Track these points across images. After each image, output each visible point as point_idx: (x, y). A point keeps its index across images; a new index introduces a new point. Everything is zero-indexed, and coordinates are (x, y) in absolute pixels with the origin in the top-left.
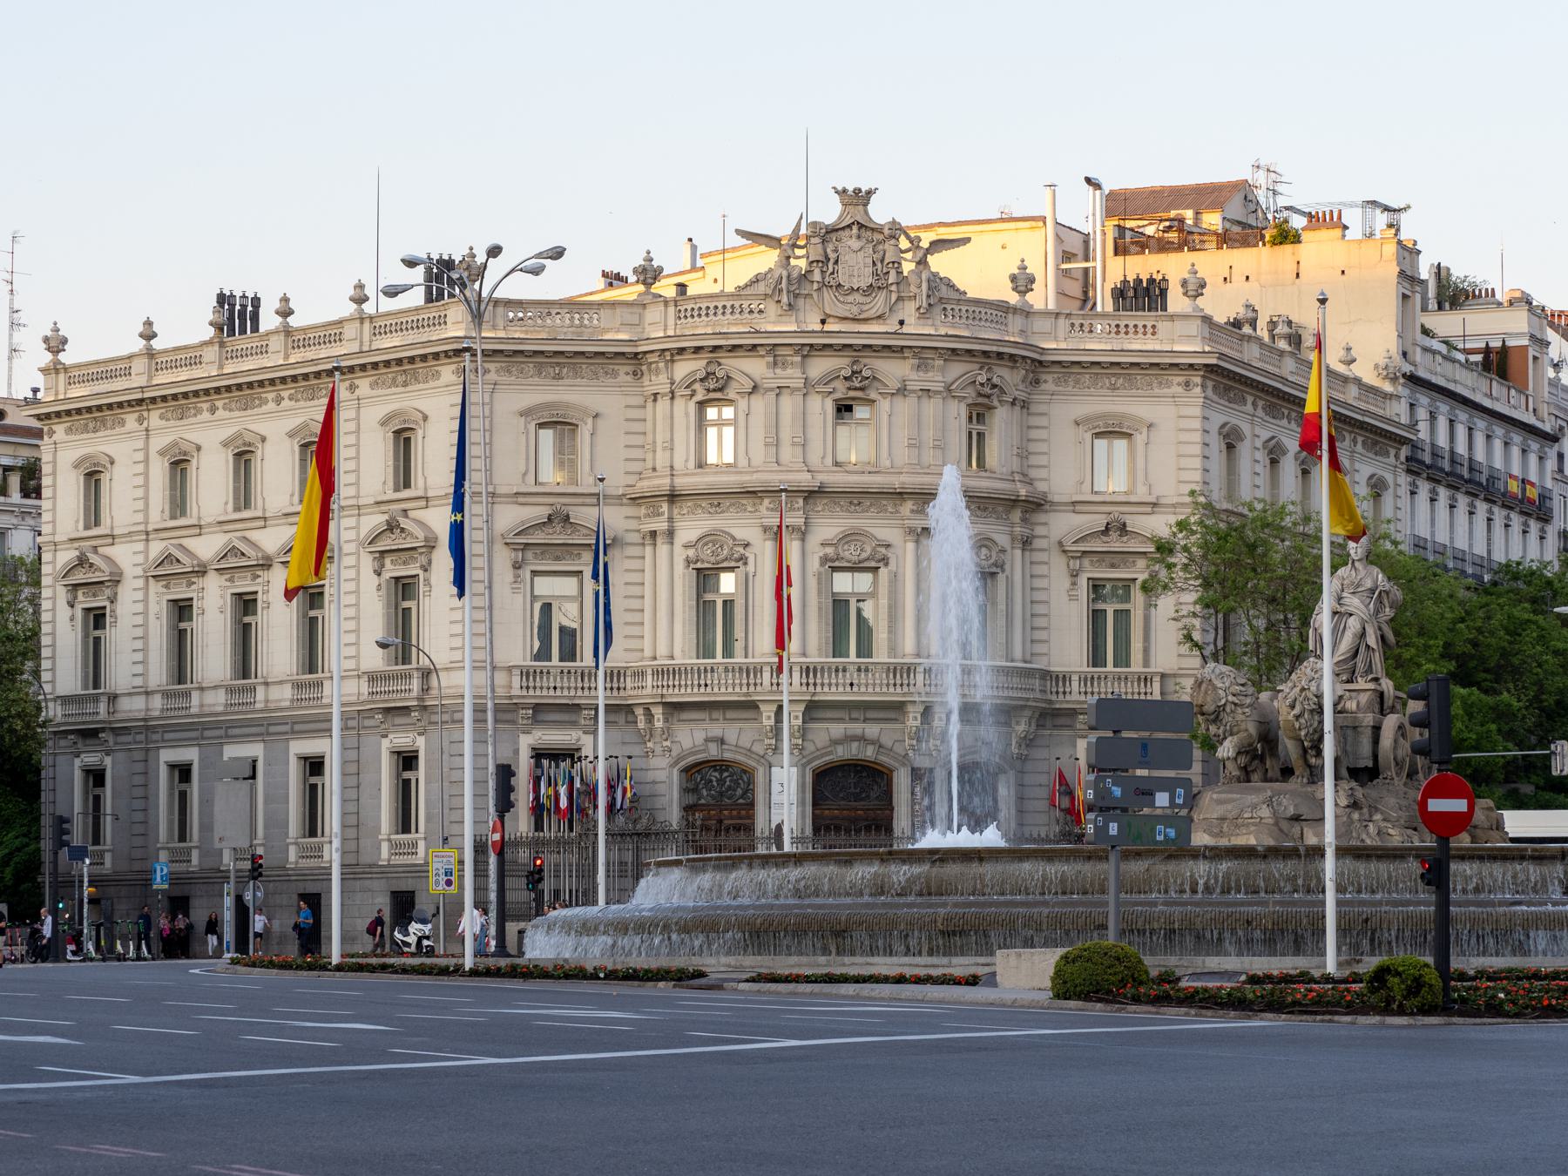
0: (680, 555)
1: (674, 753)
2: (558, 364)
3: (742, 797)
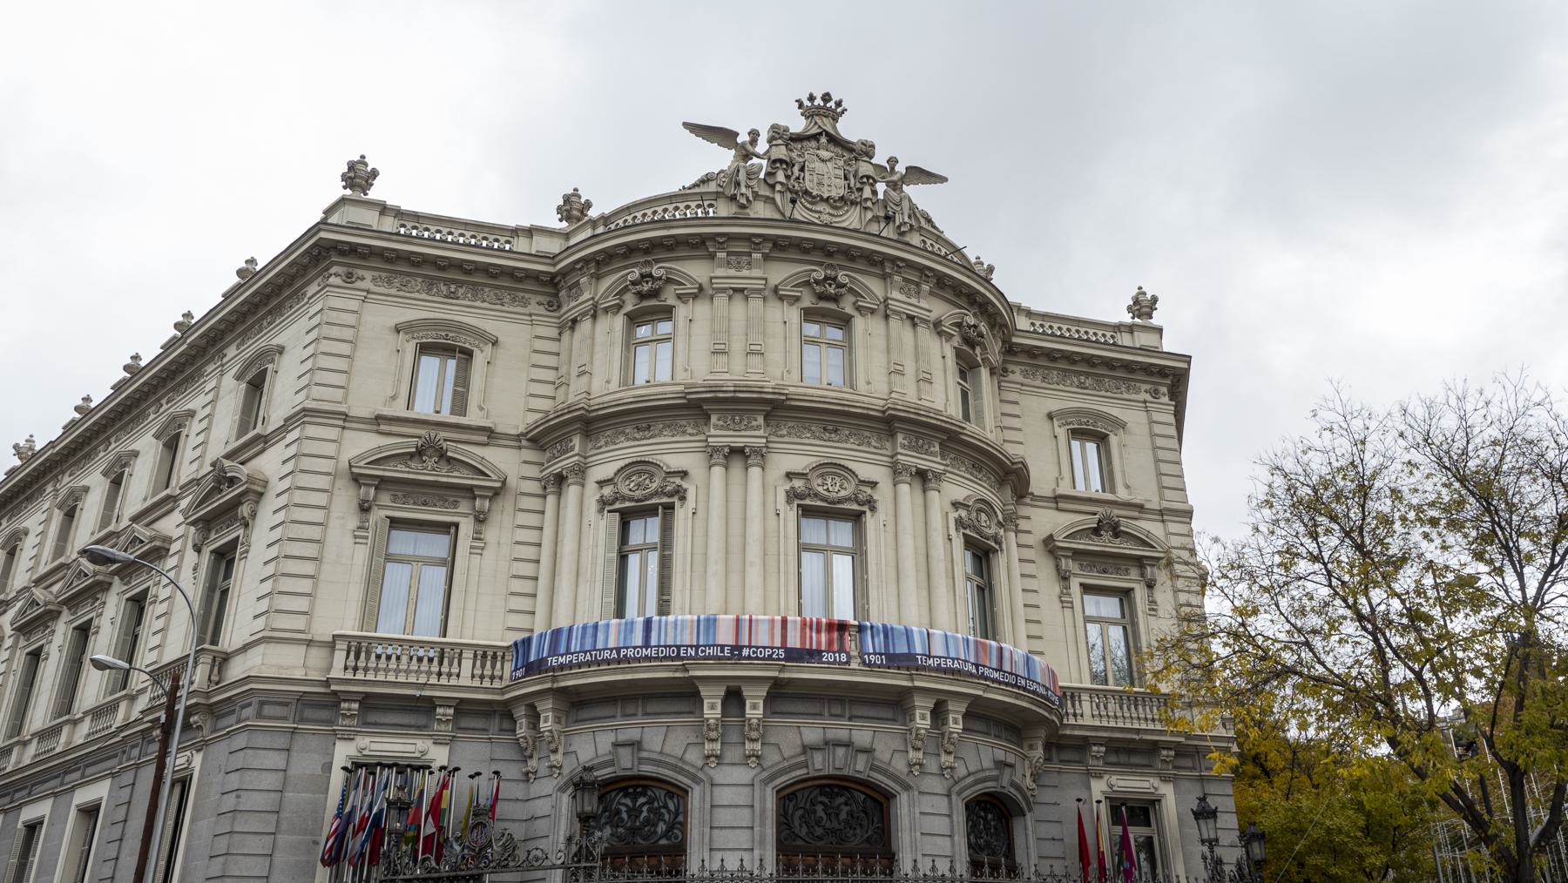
0: (592, 494)
1: (566, 771)
2: (453, 281)
3: (665, 835)
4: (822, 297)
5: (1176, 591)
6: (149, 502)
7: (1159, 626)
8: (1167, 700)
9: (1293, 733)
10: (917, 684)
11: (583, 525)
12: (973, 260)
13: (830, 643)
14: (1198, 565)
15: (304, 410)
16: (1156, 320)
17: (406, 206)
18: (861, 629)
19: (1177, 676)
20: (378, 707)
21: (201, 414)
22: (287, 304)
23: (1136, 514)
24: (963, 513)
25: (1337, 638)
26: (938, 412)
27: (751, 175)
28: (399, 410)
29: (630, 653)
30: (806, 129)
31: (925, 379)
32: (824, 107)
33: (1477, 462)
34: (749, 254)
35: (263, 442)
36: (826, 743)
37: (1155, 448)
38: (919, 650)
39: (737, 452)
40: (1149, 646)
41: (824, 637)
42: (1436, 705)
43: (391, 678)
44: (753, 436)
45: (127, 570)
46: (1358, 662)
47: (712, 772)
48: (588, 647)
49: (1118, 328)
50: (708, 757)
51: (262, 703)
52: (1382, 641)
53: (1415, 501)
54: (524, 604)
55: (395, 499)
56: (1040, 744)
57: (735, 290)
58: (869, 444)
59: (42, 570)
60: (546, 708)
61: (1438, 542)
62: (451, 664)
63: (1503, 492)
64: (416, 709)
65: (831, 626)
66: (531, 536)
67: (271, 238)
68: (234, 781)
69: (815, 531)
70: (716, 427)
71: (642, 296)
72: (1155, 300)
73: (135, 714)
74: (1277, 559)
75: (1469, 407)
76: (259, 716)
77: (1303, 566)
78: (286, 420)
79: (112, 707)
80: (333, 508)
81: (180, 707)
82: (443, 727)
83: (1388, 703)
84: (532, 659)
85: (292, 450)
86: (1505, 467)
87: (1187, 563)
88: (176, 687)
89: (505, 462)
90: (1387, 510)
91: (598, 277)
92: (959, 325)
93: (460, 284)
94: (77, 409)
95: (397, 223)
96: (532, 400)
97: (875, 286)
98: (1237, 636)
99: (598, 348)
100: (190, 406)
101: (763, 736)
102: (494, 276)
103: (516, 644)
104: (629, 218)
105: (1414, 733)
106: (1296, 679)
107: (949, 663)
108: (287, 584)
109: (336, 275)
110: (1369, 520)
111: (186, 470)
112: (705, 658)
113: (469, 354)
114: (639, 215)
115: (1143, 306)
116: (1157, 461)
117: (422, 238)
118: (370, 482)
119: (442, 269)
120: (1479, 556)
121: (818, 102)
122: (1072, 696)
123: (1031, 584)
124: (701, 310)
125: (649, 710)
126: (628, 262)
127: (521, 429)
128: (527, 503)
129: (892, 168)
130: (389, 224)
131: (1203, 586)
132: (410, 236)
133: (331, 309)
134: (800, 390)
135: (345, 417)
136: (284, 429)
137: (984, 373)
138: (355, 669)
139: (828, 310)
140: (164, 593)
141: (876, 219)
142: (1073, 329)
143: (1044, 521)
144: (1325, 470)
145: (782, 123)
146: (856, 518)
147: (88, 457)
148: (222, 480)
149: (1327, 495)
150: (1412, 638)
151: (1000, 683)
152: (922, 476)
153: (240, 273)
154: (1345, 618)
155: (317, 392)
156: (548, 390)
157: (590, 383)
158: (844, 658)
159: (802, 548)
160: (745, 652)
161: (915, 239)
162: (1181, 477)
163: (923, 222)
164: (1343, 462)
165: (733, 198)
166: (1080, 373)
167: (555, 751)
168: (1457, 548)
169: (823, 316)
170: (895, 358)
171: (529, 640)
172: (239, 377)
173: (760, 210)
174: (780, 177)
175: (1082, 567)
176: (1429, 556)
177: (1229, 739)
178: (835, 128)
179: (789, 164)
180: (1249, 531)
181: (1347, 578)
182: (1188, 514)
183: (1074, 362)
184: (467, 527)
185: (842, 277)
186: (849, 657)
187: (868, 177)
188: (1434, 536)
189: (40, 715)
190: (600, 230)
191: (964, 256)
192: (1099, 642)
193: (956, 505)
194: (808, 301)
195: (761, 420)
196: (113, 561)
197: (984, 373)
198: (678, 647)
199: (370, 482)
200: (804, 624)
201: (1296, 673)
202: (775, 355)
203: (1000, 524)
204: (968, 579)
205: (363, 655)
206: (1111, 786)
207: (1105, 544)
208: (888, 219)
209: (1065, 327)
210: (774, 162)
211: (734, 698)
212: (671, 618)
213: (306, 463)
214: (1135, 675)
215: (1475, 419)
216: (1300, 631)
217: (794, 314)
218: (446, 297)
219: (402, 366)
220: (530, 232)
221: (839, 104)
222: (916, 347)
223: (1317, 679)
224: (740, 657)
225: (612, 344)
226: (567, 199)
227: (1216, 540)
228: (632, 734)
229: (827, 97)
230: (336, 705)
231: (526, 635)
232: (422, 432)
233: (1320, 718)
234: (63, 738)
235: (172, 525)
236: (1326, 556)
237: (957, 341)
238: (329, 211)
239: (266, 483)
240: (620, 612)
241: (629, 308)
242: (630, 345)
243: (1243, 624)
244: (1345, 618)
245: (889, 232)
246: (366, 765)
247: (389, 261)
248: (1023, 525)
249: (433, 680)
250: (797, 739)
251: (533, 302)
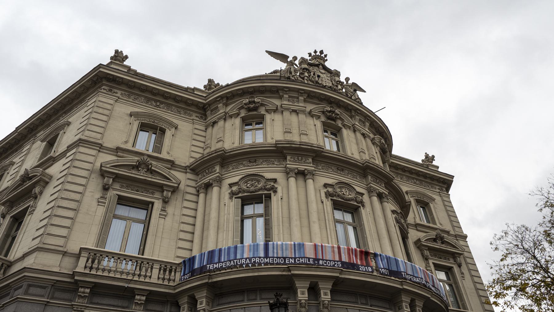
28: (129, 147)
44: (308, 166)
51: (29, 286)
55: (122, 187)
62: (146, 271)
70: (290, 161)
71: (249, 110)
76: (26, 293)
91: (226, 105)
93: (162, 103)
96: (192, 153)
99: (227, 131)
102: (177, 101)
103: (184, 261)
118: (109, 177)
119: (154, 94)
124: (277, 117)
125: (263, 297)
128: (189, 197)
138: (91, 268)
157: (223, 145)
184: (158, 205)
195: (310, 160)
199: (109, 177)
205: (96, 261)
219: (132, 130)
241: (243, 115)
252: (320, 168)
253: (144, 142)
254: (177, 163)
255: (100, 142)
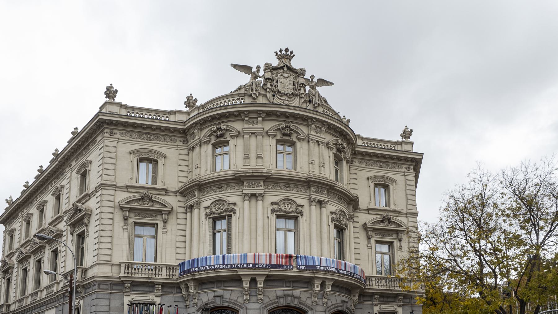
0: (203, 212)
1: (199, 305)
2: (149, 133)
4: (284, 135)
5: (409, 242)
6: (54, 218)
7: (402, 254)
8: (402, 280)
9: (445, 290)
10: (316, 276)
11: (200, 223)
12: (342, 117)
13: (286, 262)
14: (418, 233)
15: (101, 184)
16: (411, 140)
17: (129, 104)
18: (297, 257)
19: (407, 272)
20: (136, 285)
21: (66, 187)
22: (91, 145)
23: (397, 215)
24: (334, 216)
25: (466, 258)
26: (327, 178)
27: (257, 85)
29: (218, 267)
30: (279, 65)
31: (322, 166)
32: (286, 55)
33: (529, 192)
34: (257, 118)
35: (89, 196)
36: (285, 295)
37: (406, 190)
38: (317, 264)
39: (254, 195)
40: (398, 262)
41: (284, 260)
42: (498, 280)
43: (140, 276)
44: (258, 190)
45: (50, 242)
46: (472, 266)
47: (246, 305)
48: (204, 265)
49: (396, 143)
50: (245, 300)
51: (99, 284)
52: (482, 259)
53: (502, 208)
54: (182, 251)
55: (135, 215)
56: (357, 295)
57: (252, 133)
58: (301, 191)
59: (23, 242)
60: (191, 285)
61: (508, 223)
62: (159, 271)
63: (537, 203)
64: (149, 286)
65: (286, 257)
66: (182, 227)
67: (82, 121)
68: (94, 309)
69: (281, 223)
70: (246, 186)
71: (218, 137)
72: (412, 131)
73: (60, 289)
74: (448, 230)
75: (529, 171)
76: (99, 288)
77: (457, 232)
78: (96, 188)
79: (52, 286)
80: (115, 219)
81: (74, 286)
82: (158, 291)
83: (481, 280)
84: (186, 269)
85: (99, 199)
86: (539, 194)
87: (414, 232)
88: (71, 280)
89: (172, 201)
90: (490, 211)
91: (201, 130)
92: (336, 144)
94: (24, 186)
95: (126, 111)
97: (304, 129)
98: (429, 258)
99: (202, 158)
100: (62, 184)
101: (263, 293)
102: (163, 131)
104: (212, 105)
105: (489, 290)
106: (449, 272)
107: (327, 268)
108: (103, 246)
109: (107, 133)
110: (484, 215)
111: (64, 207)
112: (244, 268)
113: (156, 161)
114: (215, 104)
115: (407, 134)
116: (407, 195)
117: (136, 117)
118: (127, 210)
119: (144, 129)
120: (523, 228)
121: (284, 52)
122: (369, 279)
123: (357, 241)
124: (239, 142)
125: (225, 285)
126: (211, 123)
127: (177, 189)
129: (312, 80)
130: (124, 112)
131: (419, 240)
132: (131, 116)
133: (107, 146)
134: (276, 172)
135: (116, 186)
136: (95, 191)
137: (344, 163)
138: (128, 273)
139: (287, 139)
140: (63, 249)
141: (305, 102)
142: (379, 144)
143: (363, 218)
144: (470, 197)
145: (269, 62)
146: (296, 218)
147: (31, 203)
148: (77, 210)
149: (469, 206)
150: (493, 257)
151: (344, 275)
152: (320, 203)
153: (73, 133)
154: (470, 251)
155: (105, 177)
156: (185, 174)
158: (291, 267)
159: (277, 229)
160: (257, 266)
161: (320, 110)
162: (415, 200)
163: (323, 102)
164: (477, 194)
165: (251, 95)
166: (380, 162)
167: (195, 299)
168: (515, 225)
169: (285, 142)
170: (311, 158)
171: (184, 263)
172: (77, 173)
173: (261, 100)
174: (269, 86)
175: (376, 234)
176: (504, 228)
177: (423, 293)
178: (290, 63)
179: (272, 80)
180: (438, 220)
181: (472, 236)
182: (417, 214)
183: (379, 157)
184: (160, 225)
185: (292, 127)
186: (293, 267)
187: (303, 84)
188: (507, 220)
189: (30, 289)
190: (201, 111)
191: (339, 116)
192: (380, 260)
193: (332, 213)
194: (279, 137)
195: (262, 183)
196: (46, 239)
197: (344, 163)
198: (234, 264)
199: (127, 210)
200: (277, 256)
201: (449, 270)
202: (267, 158)
203: (347, 220)
204: (335, 239)
206: (380, 308)
207: (385, 226)
208: (310, 101)
209: (376, 144)
210: (267, 79)
211: (253, 281)
212: (232, 255)
213: (104, 203)
214: (392, 271)
215: (531, 176)
216: (452, 255)
217: (274, 142)
218: (147, 140)
219: (133, 167)
220: (175, 113)
221: (292, 53)
222: (319, 153)
223: (457, 272)
224: (256, 267)
225: (207, 156)
226: (188, 99)
227: (426, 224)
228: (220, 293)
229: (287, 50)
230: (123, 285)
231: (183, 261)
232: (142, 191)
233: (456, 285)
234: (39, 296)
235: (62, 226)
236: (466, 229)
237: (335, 150)
238: (101, 108)
239: (91, 211)
240: (214, 253)
241: (213, 142)
242: (214, 156)
243: (433, 254)
244: (470, 251)
245: (310, 107)
246: (135, 303)
247: (125, 126)
248: (356, 219)
249: (154, 276)
250: (275, 294)
251: (178, 140)
252: (270, 188)
253: (144, 177)
254: (169, 190)
255: (114, 183)
